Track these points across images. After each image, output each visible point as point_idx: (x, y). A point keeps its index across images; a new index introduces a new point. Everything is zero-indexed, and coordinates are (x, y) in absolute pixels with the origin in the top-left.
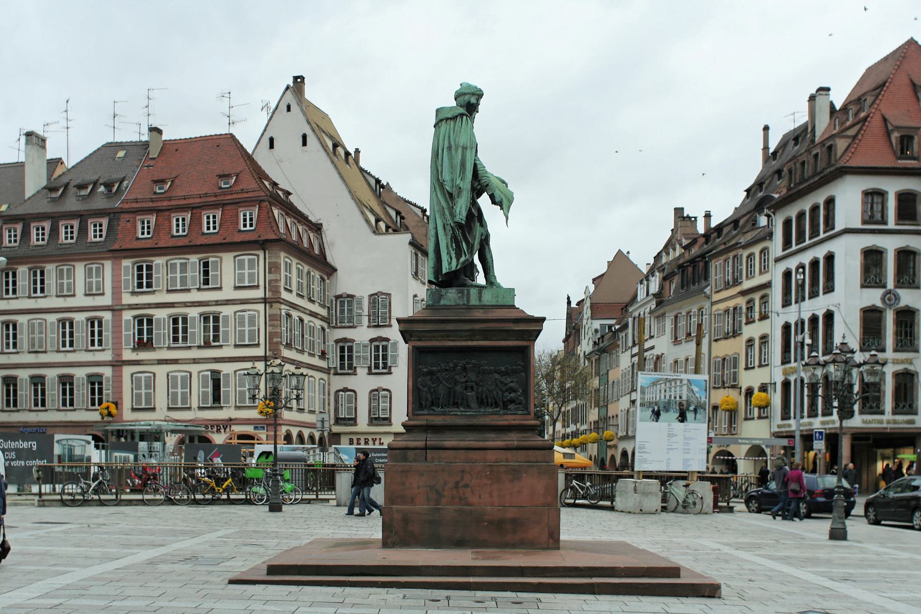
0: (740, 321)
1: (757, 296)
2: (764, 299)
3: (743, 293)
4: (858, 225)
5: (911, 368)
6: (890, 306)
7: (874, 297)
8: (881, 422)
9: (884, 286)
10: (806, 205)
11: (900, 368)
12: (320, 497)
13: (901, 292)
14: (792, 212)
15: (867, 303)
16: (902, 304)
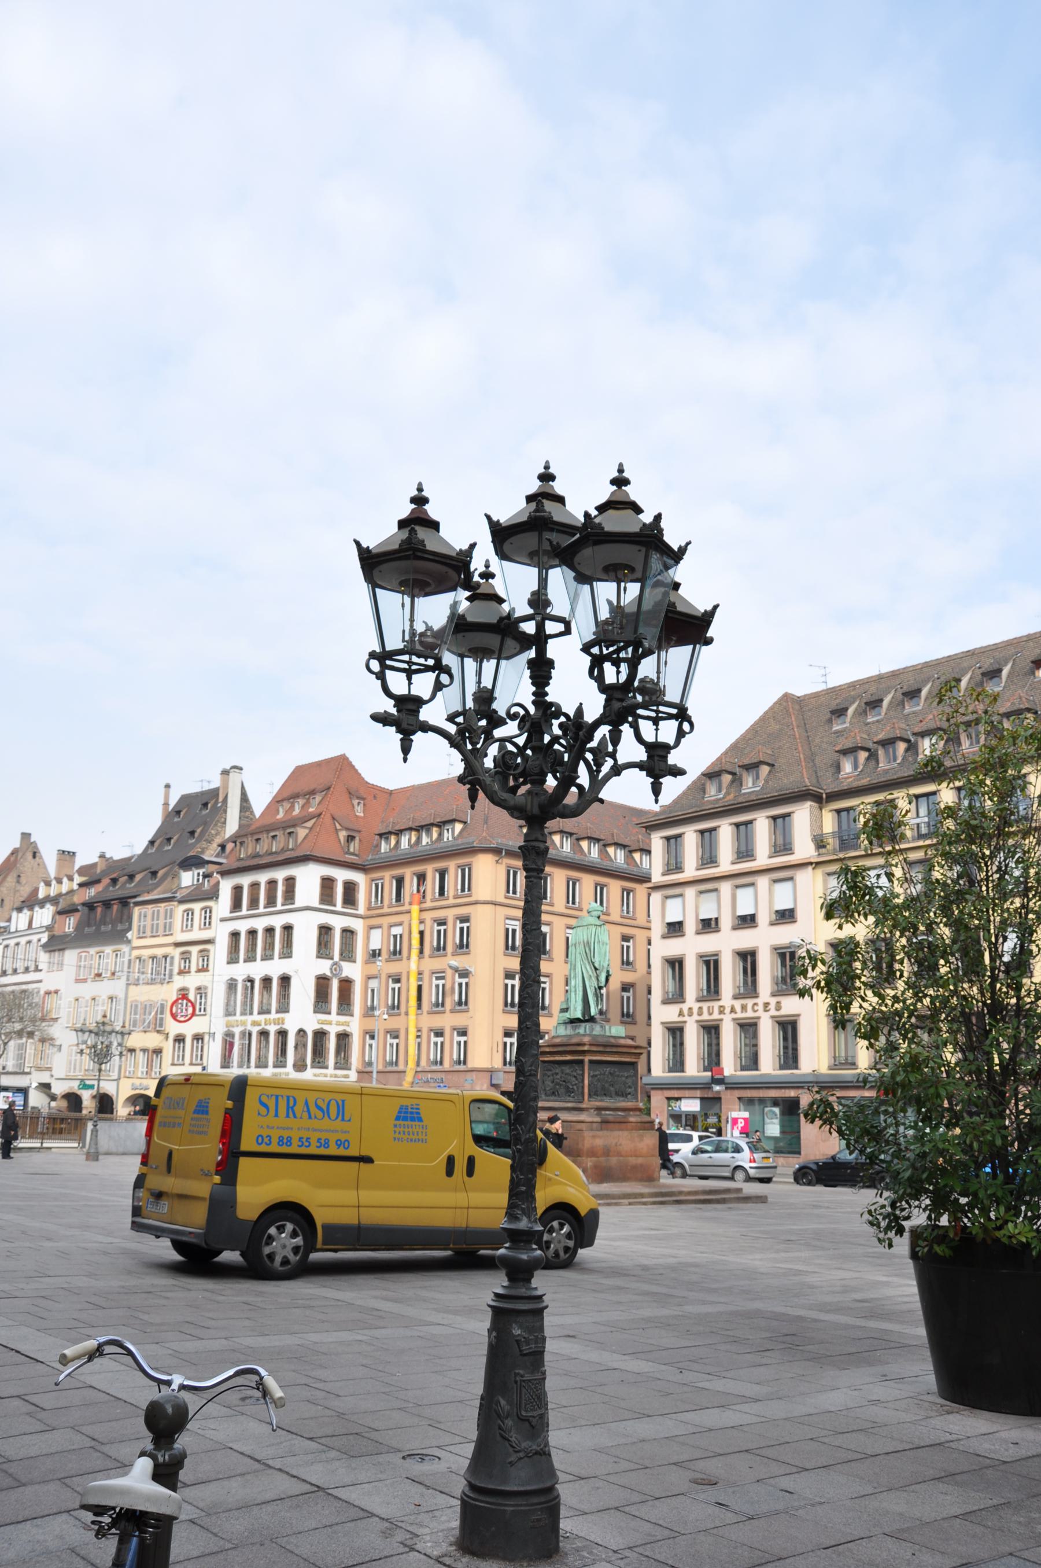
0: (171, 971)
1: (194, 950)
2: (204, 954)
3: (177, 945)
4: (316, 904)
5: (348, 1029)
6: (335, 975)
7: (324, 967)
8: (326, 1076)
9: (332, 959)
10: (263, 878)
11: (340, 1029)
12: (45, 1145)
13: (343, 964)
14: (245, 881)
15: (320, 972)
16: (344, 975)
